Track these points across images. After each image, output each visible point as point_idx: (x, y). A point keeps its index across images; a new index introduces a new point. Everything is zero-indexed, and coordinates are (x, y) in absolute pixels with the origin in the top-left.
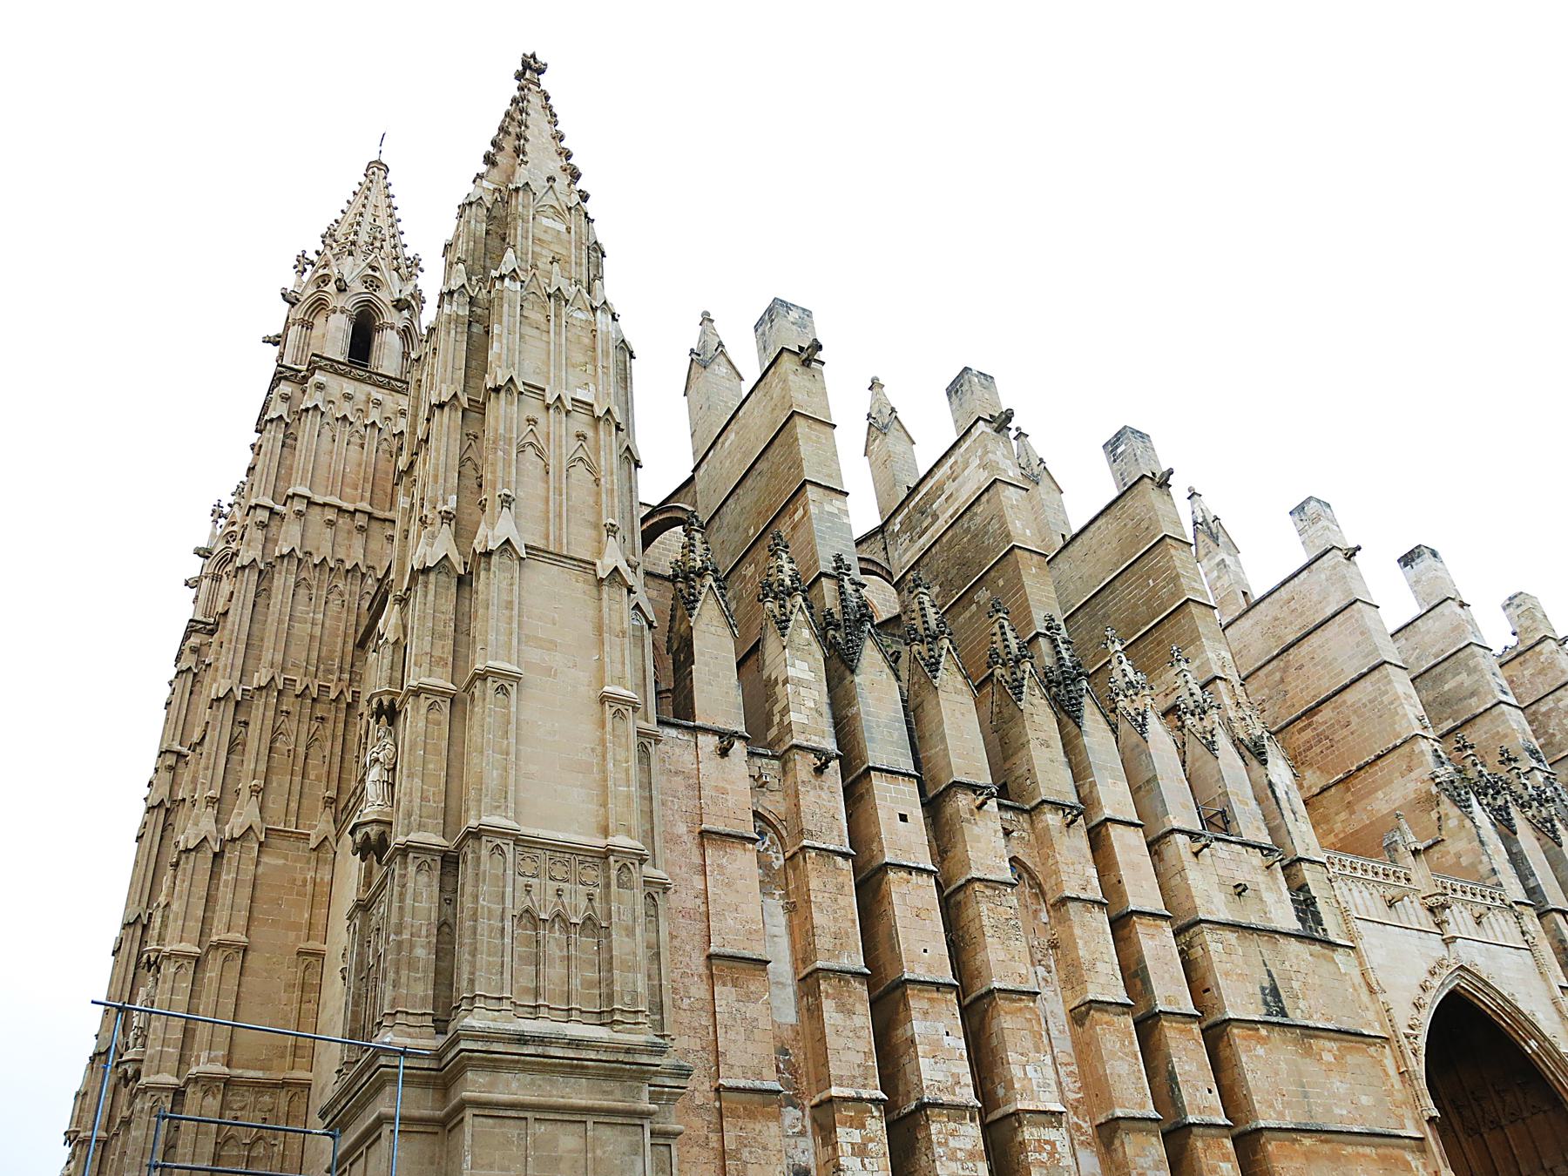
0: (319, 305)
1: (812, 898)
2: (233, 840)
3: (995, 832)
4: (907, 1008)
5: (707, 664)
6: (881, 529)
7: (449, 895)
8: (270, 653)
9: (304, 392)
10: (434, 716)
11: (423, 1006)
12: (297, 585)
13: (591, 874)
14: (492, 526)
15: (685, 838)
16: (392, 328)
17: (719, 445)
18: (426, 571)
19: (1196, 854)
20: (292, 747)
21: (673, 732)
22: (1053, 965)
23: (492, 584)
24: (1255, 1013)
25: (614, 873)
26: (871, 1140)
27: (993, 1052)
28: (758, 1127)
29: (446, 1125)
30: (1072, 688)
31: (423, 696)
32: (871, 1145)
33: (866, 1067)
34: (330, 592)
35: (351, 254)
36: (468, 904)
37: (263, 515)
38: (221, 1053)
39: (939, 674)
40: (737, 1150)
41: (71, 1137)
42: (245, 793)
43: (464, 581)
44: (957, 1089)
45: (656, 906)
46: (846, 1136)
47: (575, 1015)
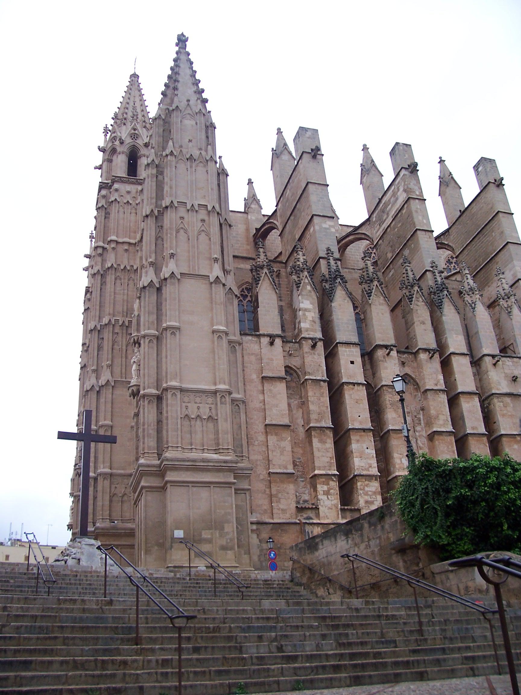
0: (114, 151)
1: (309, 399)
2: (102, 386)
3: (395, 364)
4: (351, 440)
5: (264, 307)
6: (368, 220)
7: (160, 412)
8: (108, 309)
9: (110, 193)
10: (151, 344)
11: (154, 450)
12: (116, 279)
13: (210, 400)
14: (167, 267)
15: (256, 380)
16: (144, 156)
17: (284, 195)
18: (144, 287)
19: (495, 365)
20: (120, 347)
21: (250, 338)
22: (422, 417)
23: (168, 290)
24: (515, 430)
25: (218, 399)
26: (332, 489)
27: (390, 453)
28: (285, 486)
29: (163, 489)
30: (441, 294)
31: (146, 338)
32: (331, 491)
33: (331, 463)
34: (129, 280)
35: (125, 124)
36: (165, 415)
37: (100, 251)
38: (108, 464)
39: (371, 298)
40: (276, 494)
41: (71, 494)
42: (105, 367)
43: (159, 290)
44: (370, 469)
45: (239, 409)
46: (321, 488)
47: (206, 451)
